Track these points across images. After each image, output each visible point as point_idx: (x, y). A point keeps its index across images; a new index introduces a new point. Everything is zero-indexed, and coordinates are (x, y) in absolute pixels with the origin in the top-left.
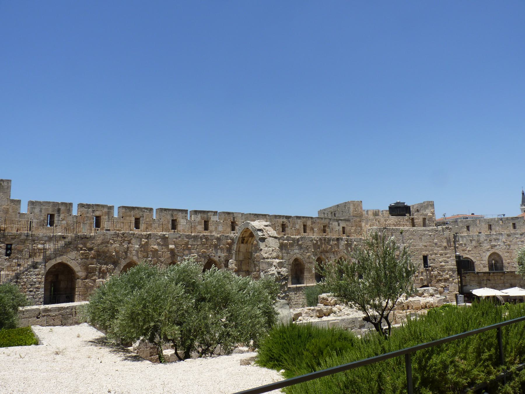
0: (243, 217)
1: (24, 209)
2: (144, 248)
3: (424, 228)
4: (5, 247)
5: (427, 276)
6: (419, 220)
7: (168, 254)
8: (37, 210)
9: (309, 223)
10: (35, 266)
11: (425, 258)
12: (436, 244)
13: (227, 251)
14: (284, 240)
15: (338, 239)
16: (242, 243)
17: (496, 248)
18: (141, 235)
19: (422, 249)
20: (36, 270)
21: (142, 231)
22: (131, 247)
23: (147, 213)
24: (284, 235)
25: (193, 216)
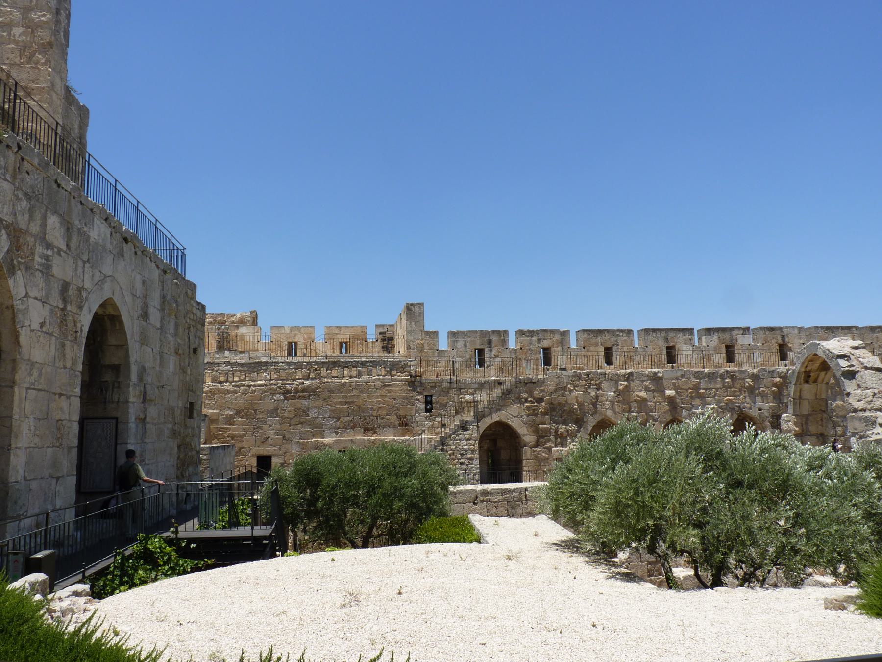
0: (803, 334)
1: (443, 344)
2: (623, 395)
4: (423, 400)
7: (665, 406)
8: (460, 344)
10: (464, 427)
13: (774, 398)
16: (807, 382)
18: (617, 374)
20: (467, 432)
21: (617, 369)
22: (602, 395)
23: (622, 339)
25: (703, 338)
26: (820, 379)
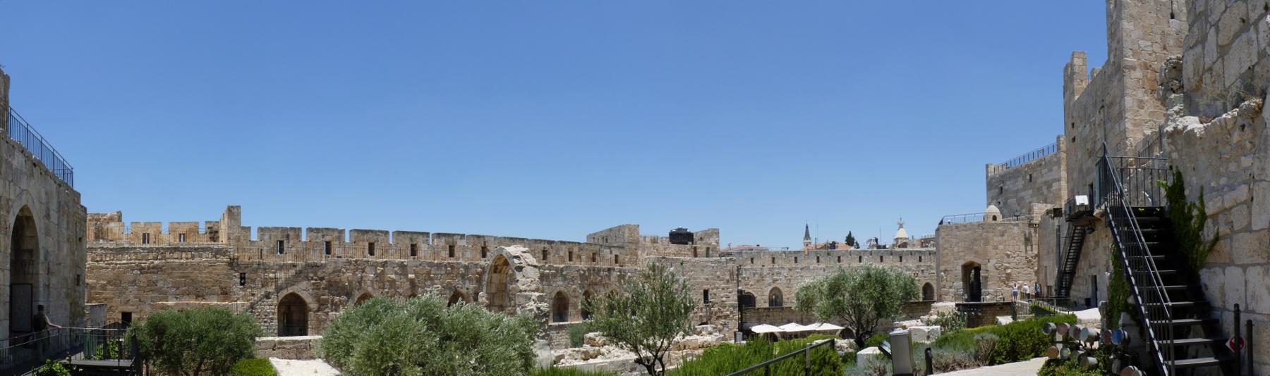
0: (497, 242)
2: (380, 277)
3: (707, 259)
5: (707, 312)
6: (702, 250)
7: (407, 285)
9: (576, 250)
10: (267, 296)
11: (706, 293)
12: (718, 277)
13: (477, 282)
14: (545, 270)
15: (609, 270)
16: (495, 272)
17: (779, 281)
18: (376, 262)
19: (703, 283)
20: (270, 300)
21: (377, 259)
22: (366, 276)
23: (382, 237)
24: (546, 263)
25: (435, 240)
26: (503, 271)
